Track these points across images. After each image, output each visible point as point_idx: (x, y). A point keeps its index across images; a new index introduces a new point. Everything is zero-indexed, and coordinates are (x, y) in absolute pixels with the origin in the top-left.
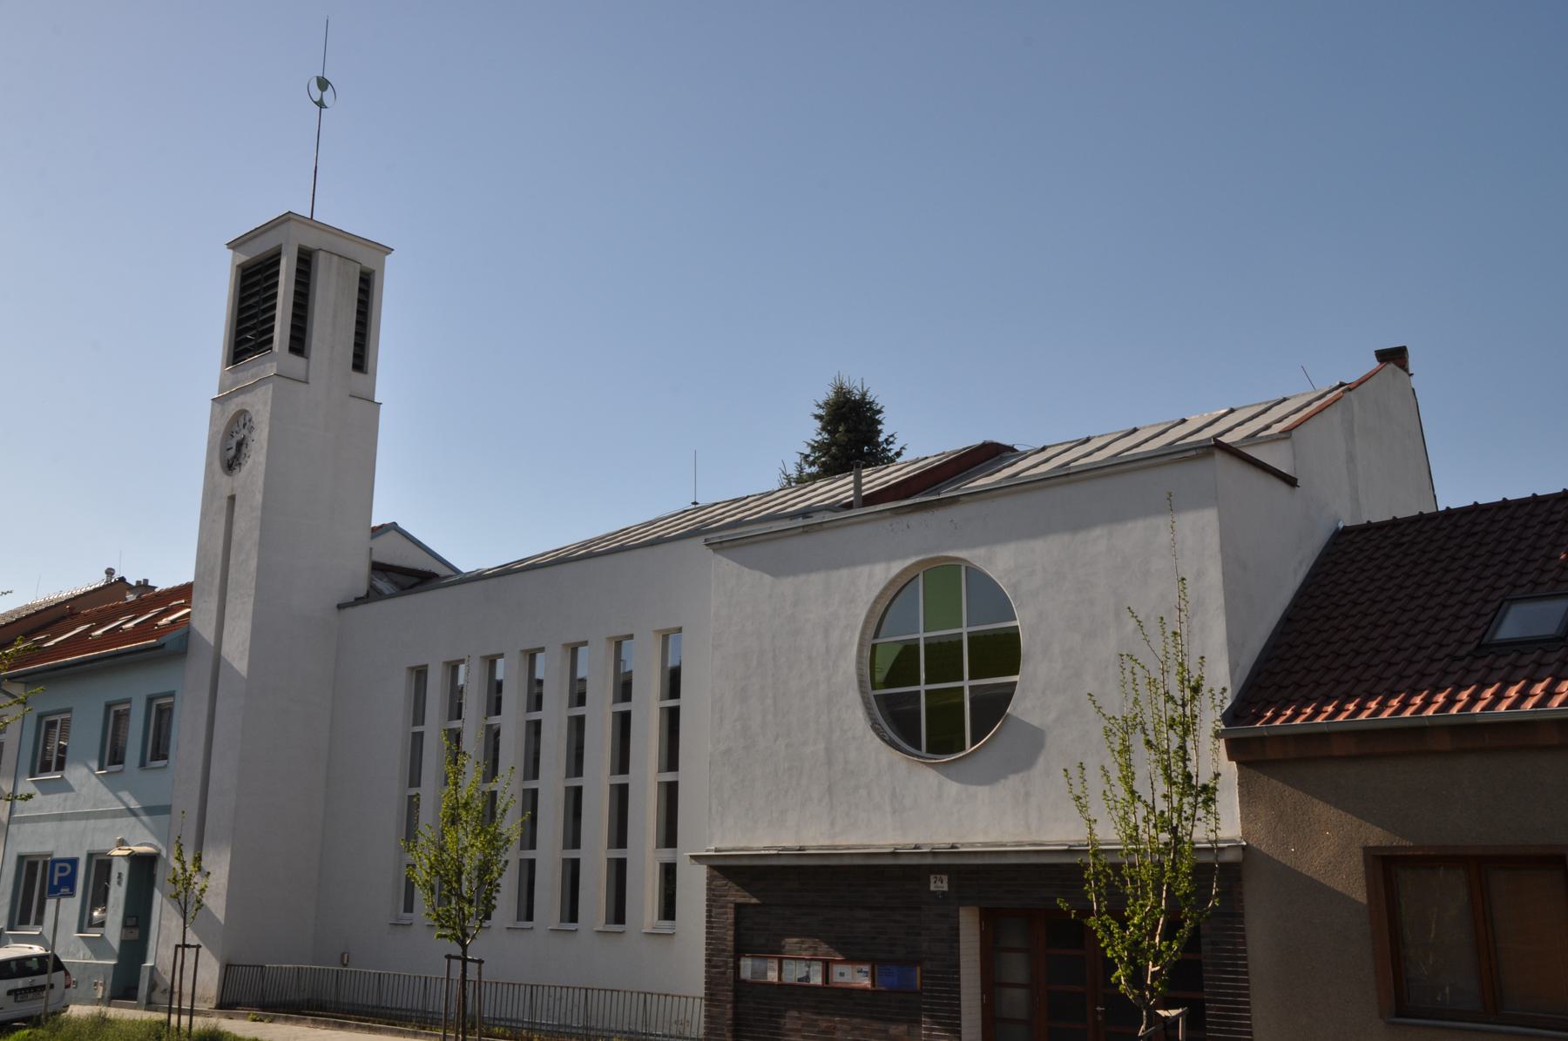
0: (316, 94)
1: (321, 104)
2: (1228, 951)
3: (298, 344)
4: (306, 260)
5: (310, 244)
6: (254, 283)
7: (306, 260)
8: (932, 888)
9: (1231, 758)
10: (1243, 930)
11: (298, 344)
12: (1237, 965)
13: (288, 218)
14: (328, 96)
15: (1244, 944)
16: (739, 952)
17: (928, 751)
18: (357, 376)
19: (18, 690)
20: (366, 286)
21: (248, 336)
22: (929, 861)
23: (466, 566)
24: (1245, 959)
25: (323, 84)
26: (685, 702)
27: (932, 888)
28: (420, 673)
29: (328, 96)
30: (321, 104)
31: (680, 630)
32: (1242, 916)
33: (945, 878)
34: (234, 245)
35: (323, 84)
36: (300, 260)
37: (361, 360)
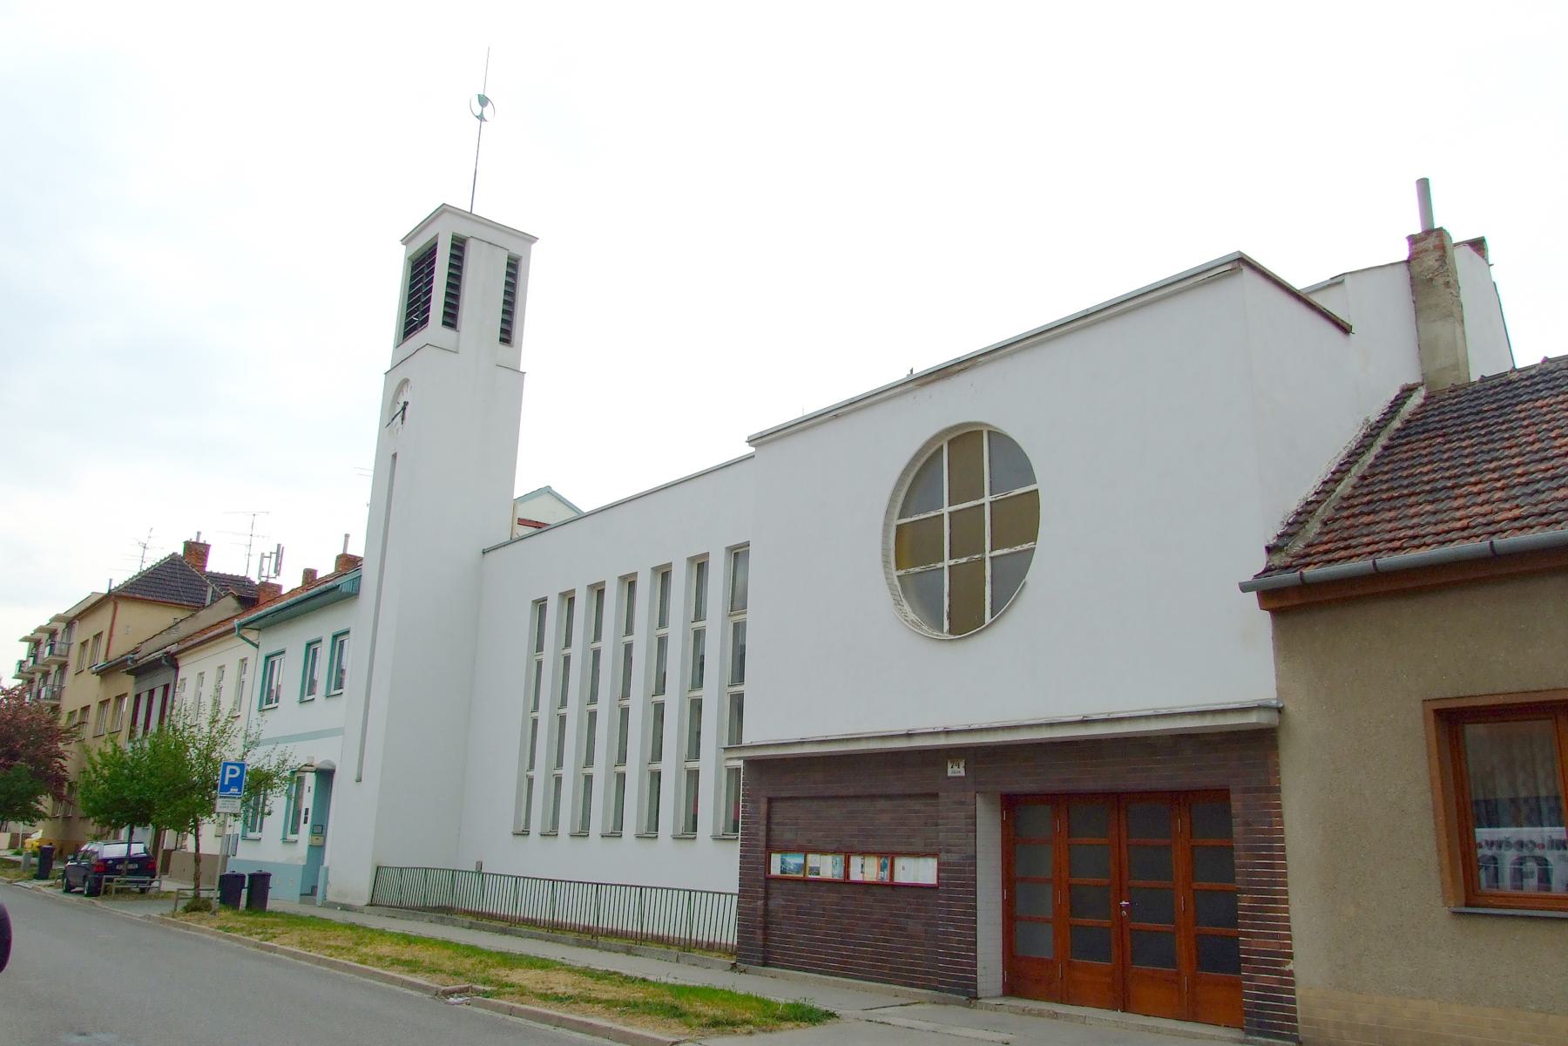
0: (478, 109)
1: (481, 118)
2: (1262, 832)
3: (451, 320)
4: (459, 246)
5: (463, 230)
6: (420, 267)
7: (459, 246)
8: (950, 774)
9: (1263, 607)
10: (1279, 806)
11: (451, 320)
12: (1271, 848)
13: (444, 210)
14: (488, 111)
15: (1282, 823)
16: (770, 849)
17: (950, 632)
18: (503, 348)
19: (252, 636)
20: (513, 268)
21: (414, 317)
22: (942, 741)
23: (586, 508)
24: (1282, 840)
25: (483, 101)
26: (752, 617)
27: (950, 774)
28: (541, 605)
29: (488, 111)
30: (481, 118)
31: (748, 544)
32: (1279, 790)
33: (962, 764)
34: (406, 241)
35: (483, 101)
36: (453, 246)
37: (506, 336)
